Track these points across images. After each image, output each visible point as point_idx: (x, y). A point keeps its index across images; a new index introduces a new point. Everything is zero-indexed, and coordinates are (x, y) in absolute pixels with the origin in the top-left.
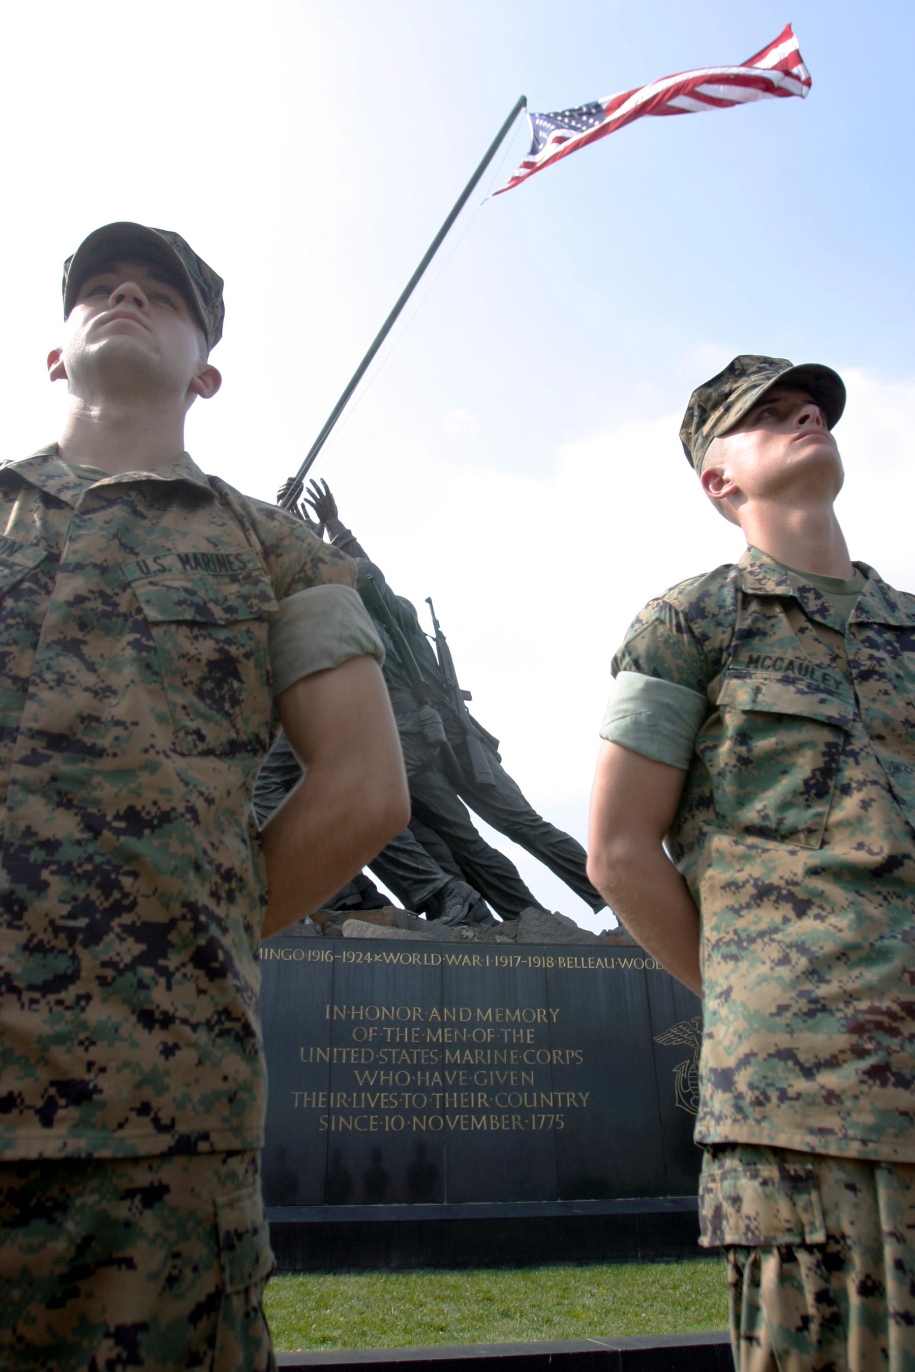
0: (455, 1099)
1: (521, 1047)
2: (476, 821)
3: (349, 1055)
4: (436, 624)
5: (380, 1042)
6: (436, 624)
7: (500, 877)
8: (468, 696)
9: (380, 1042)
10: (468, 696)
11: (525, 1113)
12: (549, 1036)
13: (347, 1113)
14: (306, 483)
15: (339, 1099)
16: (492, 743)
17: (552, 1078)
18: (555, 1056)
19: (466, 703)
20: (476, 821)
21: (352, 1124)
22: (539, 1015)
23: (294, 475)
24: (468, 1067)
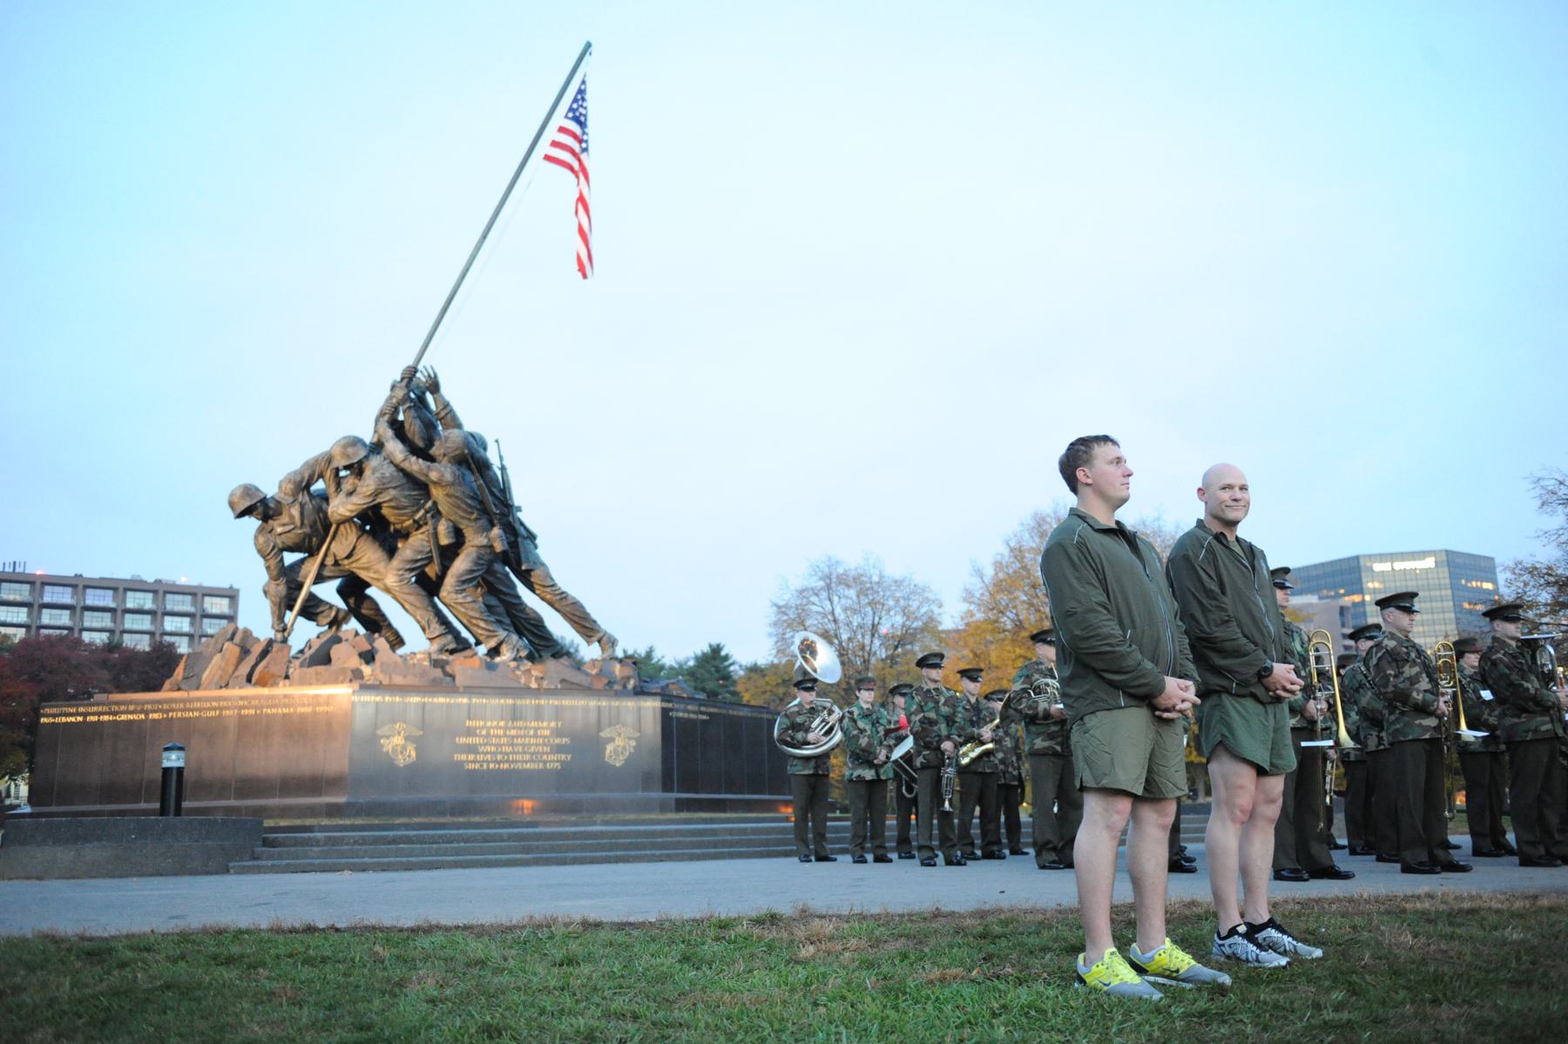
0: (519, 757)
1: (544, 737)
2: (522, 590)
3: (477, 740)
4: (501, 458)
5: (488, 735)
6: (501, 458)
7: (535, 626)
8: (519, 509)
9: (488, 735)
10: (519, 509)
11: (545, 762)
12: (558, 733)
13: (474, 762)
14: (420, 367)
15: (471, 757)
16: (532, 537)
17: (559, 749)
18: (558, 741)
19: (519, 515)
20: (522, 590)
21: (477, 766)
22: (553, 724)
23: (410, 362)
24: (524, 745)
